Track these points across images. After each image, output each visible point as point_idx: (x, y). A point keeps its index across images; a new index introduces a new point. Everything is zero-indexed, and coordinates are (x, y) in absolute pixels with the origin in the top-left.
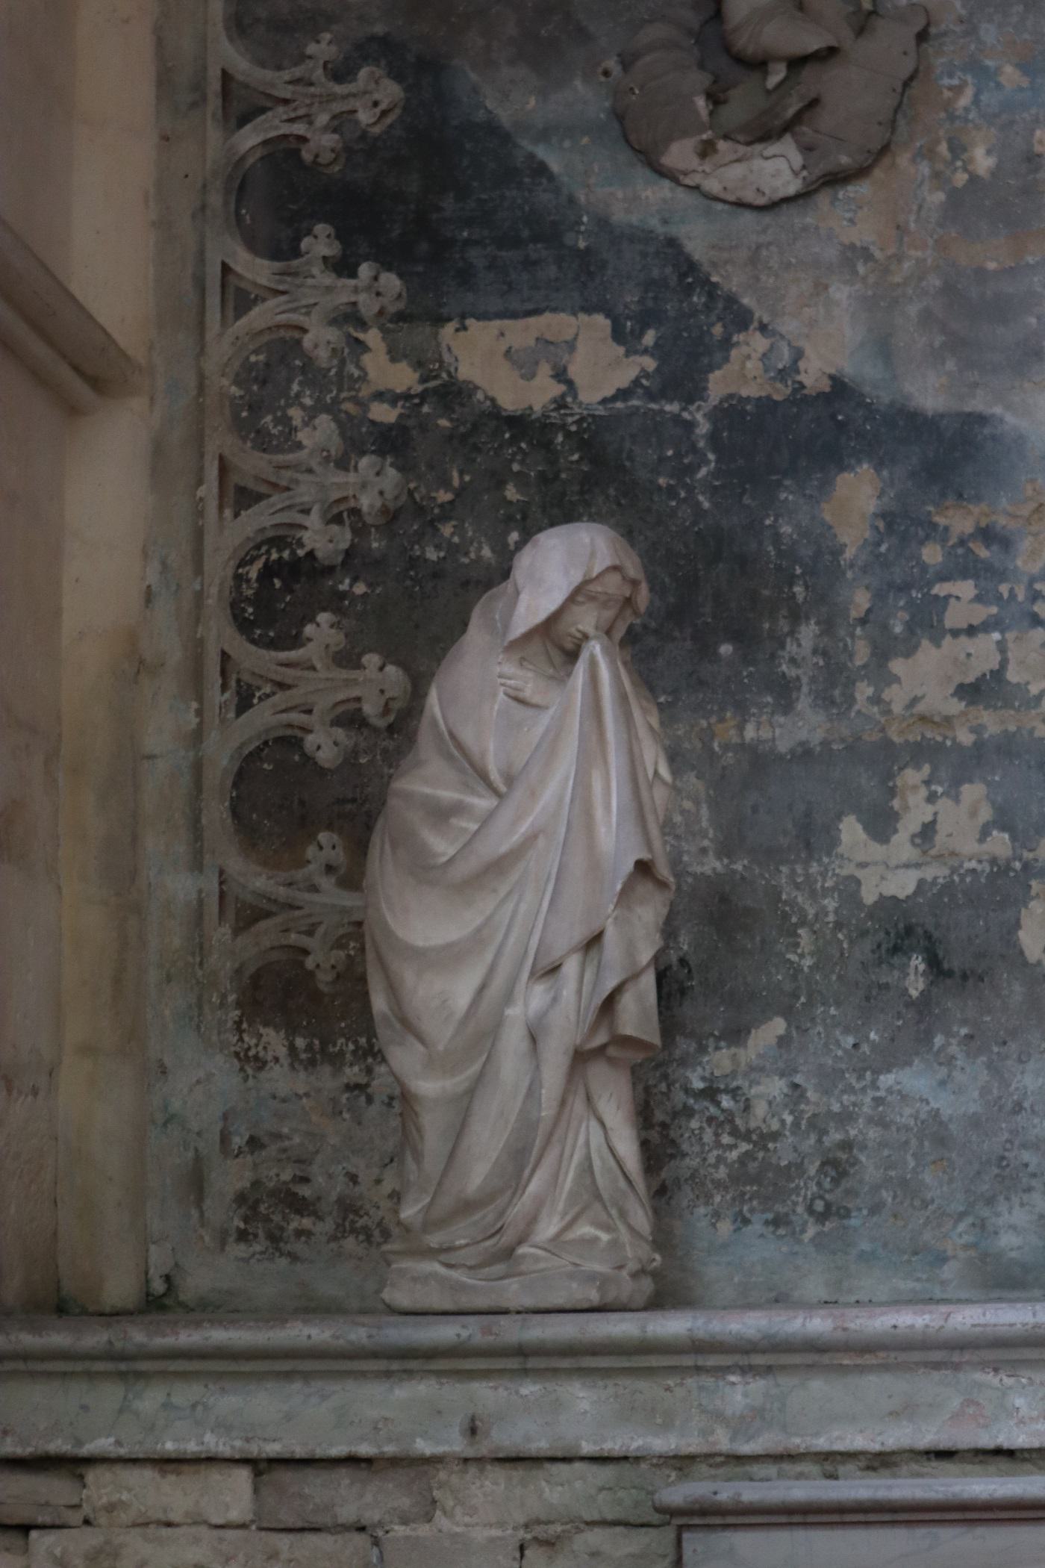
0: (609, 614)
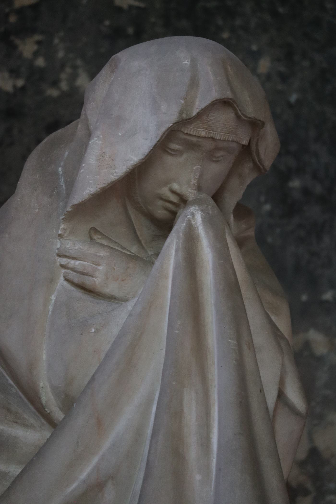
0: (216, 170)
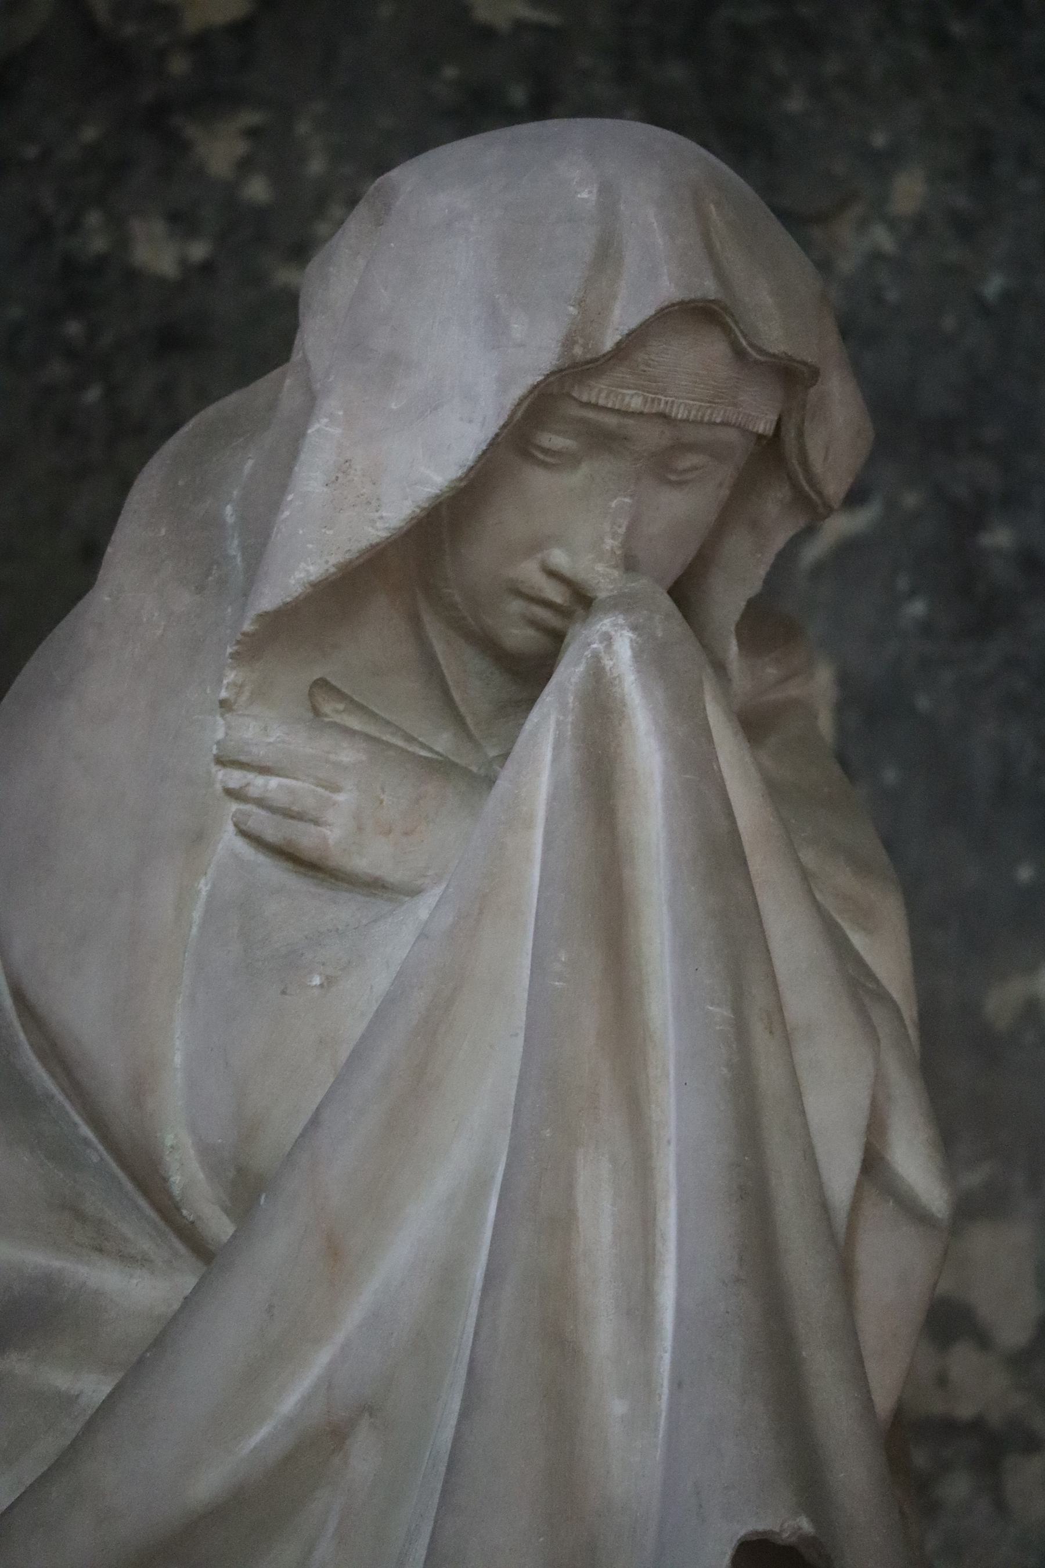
0: (680, 509)
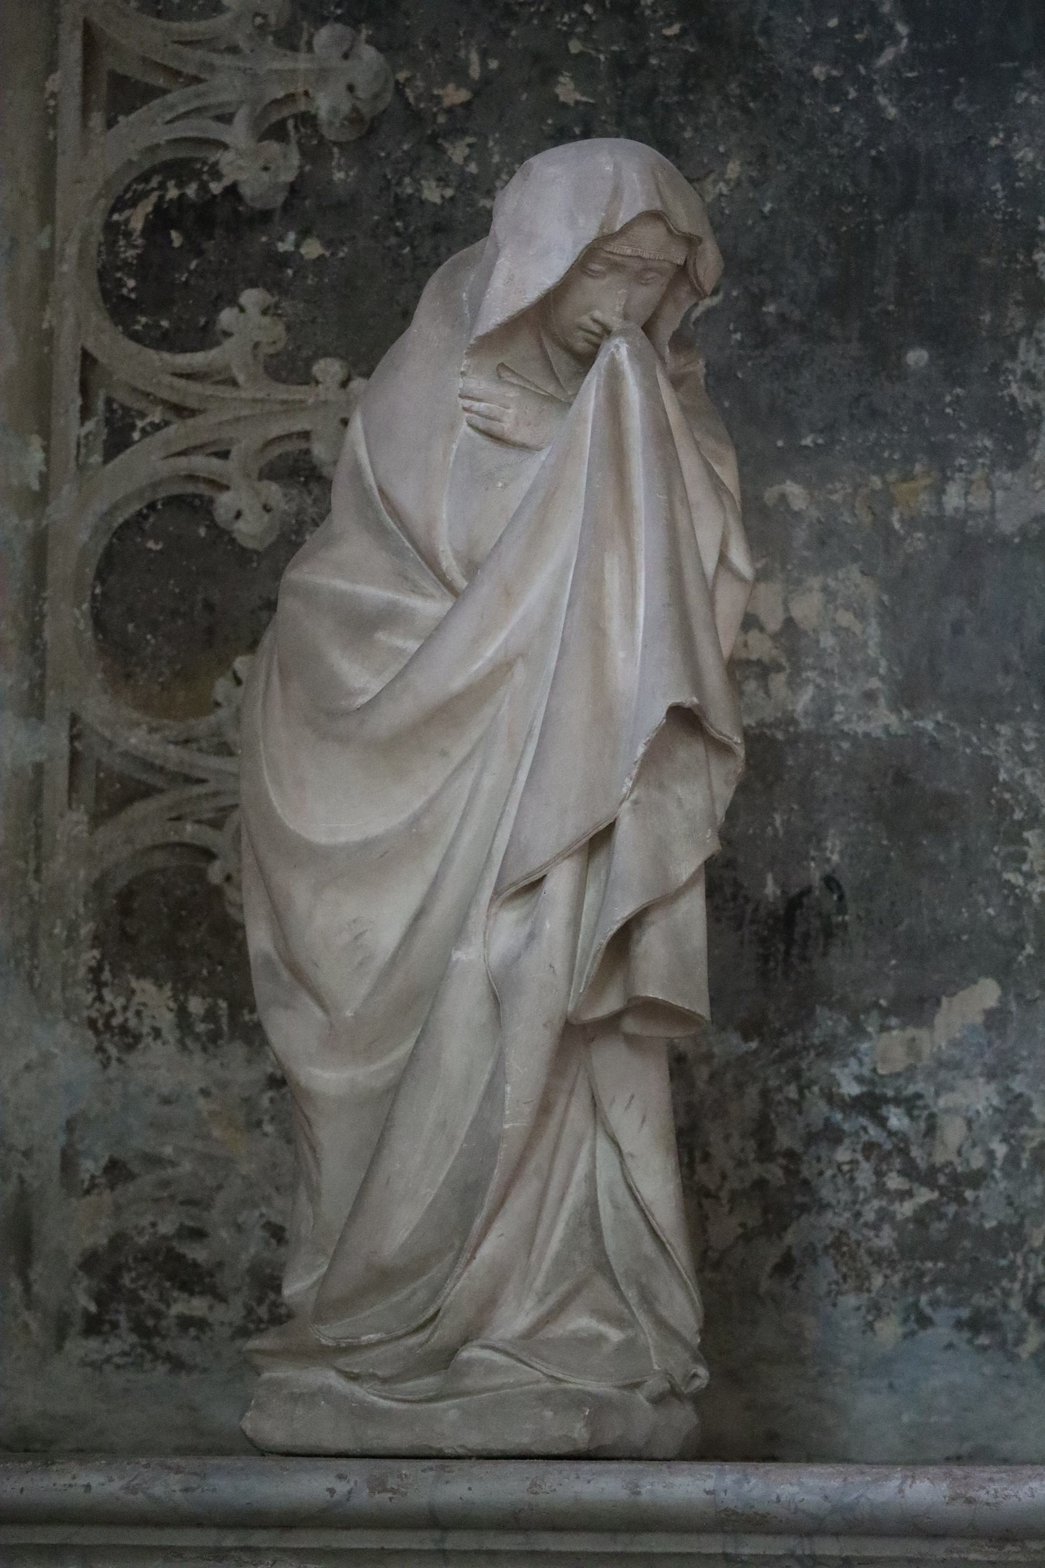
0: (647, 294)
